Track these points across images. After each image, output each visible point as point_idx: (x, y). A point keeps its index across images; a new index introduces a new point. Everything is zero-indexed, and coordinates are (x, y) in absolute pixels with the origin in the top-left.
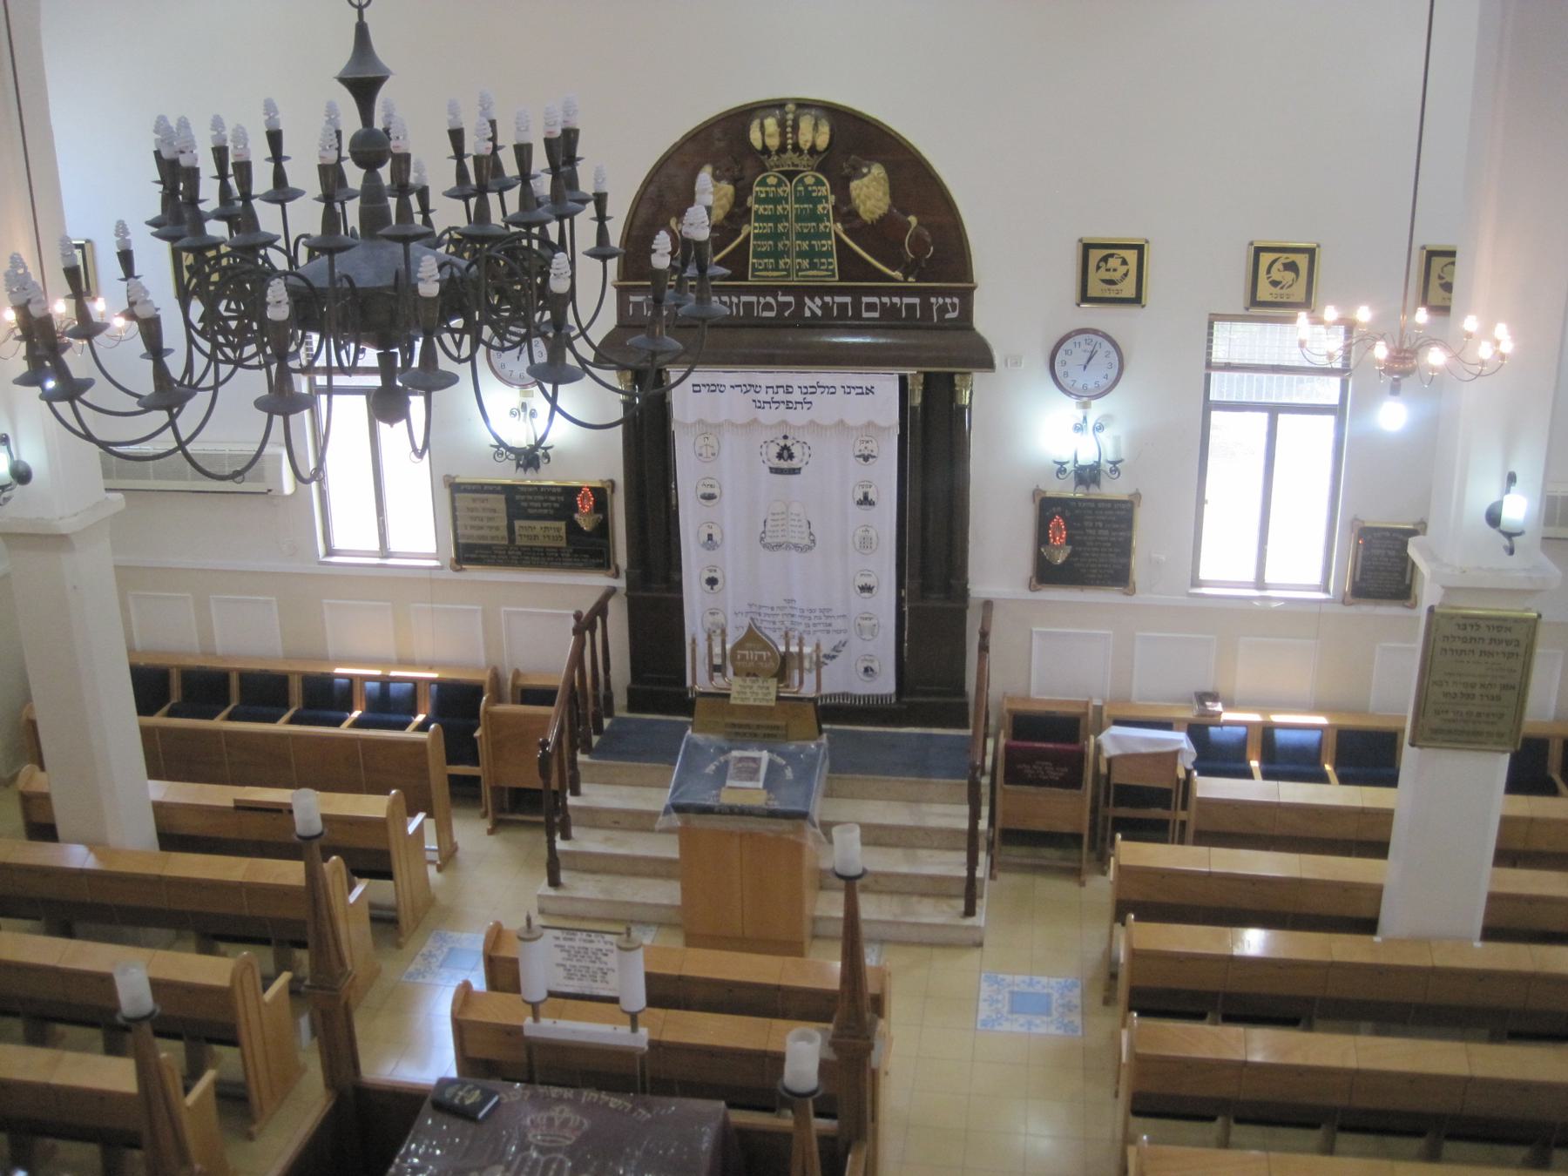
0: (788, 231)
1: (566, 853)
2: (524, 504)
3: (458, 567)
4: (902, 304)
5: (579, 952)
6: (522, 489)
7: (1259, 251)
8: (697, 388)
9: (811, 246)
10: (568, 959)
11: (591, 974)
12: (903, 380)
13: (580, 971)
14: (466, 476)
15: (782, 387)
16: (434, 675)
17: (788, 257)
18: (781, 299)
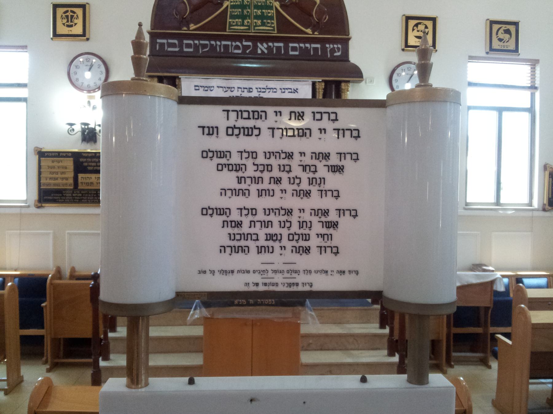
0: (250, 3)
1: (107, 368)
2: (86, 164)
3: (40, 205)
4: (311, 47)
5: (269, 168)
6: (84, 155)
7: (492, 23)
8: (197, 88)
9: (262, 13)
10: (236, 192)
11: (295, 228)
12: (314, 84)
13: (267, 224)
14: (48, 147)
15: (246, 88)
16: (18, 273)
17: (249, 19)
18: (245, 43)
